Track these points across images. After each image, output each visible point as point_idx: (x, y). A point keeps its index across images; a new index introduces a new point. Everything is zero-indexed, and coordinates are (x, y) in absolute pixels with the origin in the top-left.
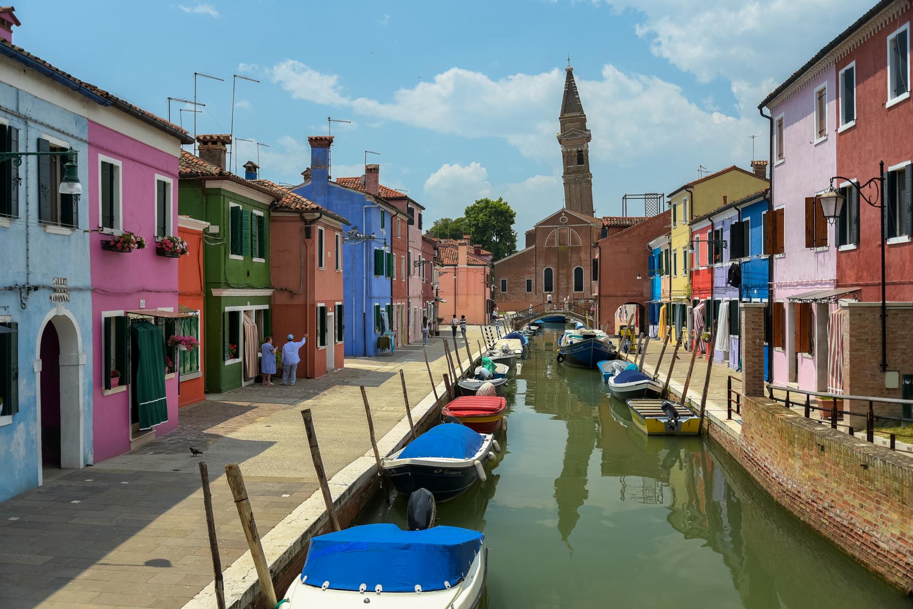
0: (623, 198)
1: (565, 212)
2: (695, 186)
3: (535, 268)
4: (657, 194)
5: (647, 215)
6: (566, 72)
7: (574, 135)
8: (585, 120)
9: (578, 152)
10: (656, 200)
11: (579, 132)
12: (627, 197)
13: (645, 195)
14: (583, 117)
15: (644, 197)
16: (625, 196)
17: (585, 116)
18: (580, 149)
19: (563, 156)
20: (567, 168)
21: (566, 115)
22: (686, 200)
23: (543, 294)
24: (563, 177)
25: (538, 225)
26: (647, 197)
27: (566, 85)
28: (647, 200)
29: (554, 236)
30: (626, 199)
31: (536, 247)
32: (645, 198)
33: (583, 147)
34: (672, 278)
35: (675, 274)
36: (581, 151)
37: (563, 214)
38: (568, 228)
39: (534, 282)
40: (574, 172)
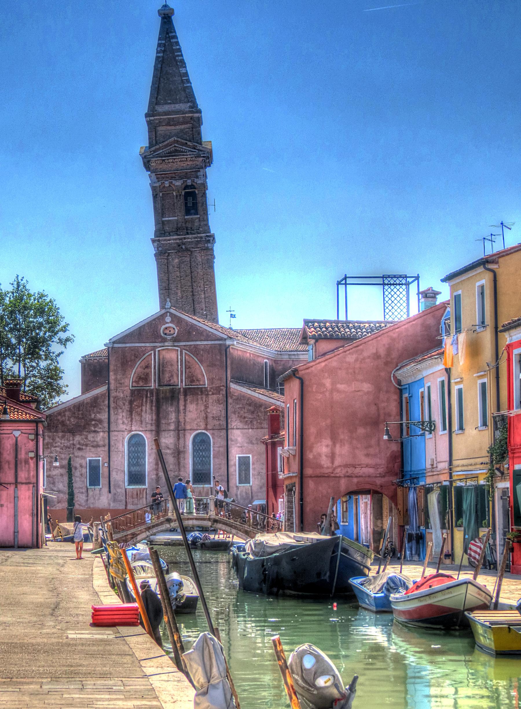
0: (339, 283)
1: (172, 315)
2: (501, 260)
3: (106, 435)
4: (406, 277)
5: (387, 317)
6: (160, 18)
7: (176, 151)
8: (199, 121)
9: (186, 187)
10: (404, 287)
11: (189, 146)
12: (349, 281)
13: (383, 277)
14: (196, 115)
15: (380, 281)
16: (345, 278)
17: (200, 112)
18: (189, 182)
19: (155, 197)
20: (163, 222)
21: (160, 109)
22: (482, 287)
23: (126, 489)
24: (153, 241)
25: (114, 343)
26: (386, 282)
27: (159, 45)
28: (386, 287)
29: (148, 367)
30: (346, 284)
31: (109, 390)
32: (384, 284)
33: (197, 177)
34: (454, 435)
35: (461, 428)
36: (192, 187)
37: (168, 319)
38: (179, 349)
39: (106, 465)
40: (177, 230)
